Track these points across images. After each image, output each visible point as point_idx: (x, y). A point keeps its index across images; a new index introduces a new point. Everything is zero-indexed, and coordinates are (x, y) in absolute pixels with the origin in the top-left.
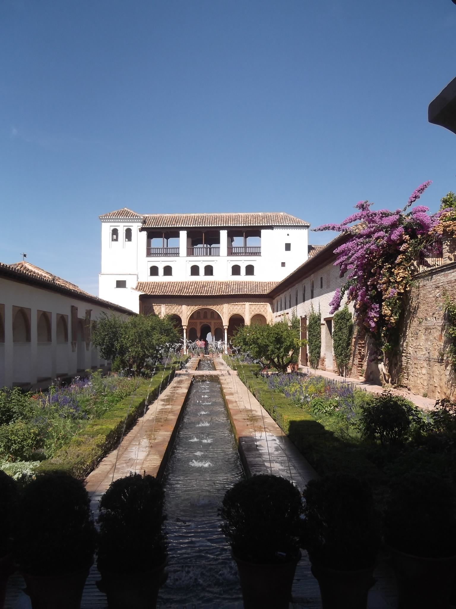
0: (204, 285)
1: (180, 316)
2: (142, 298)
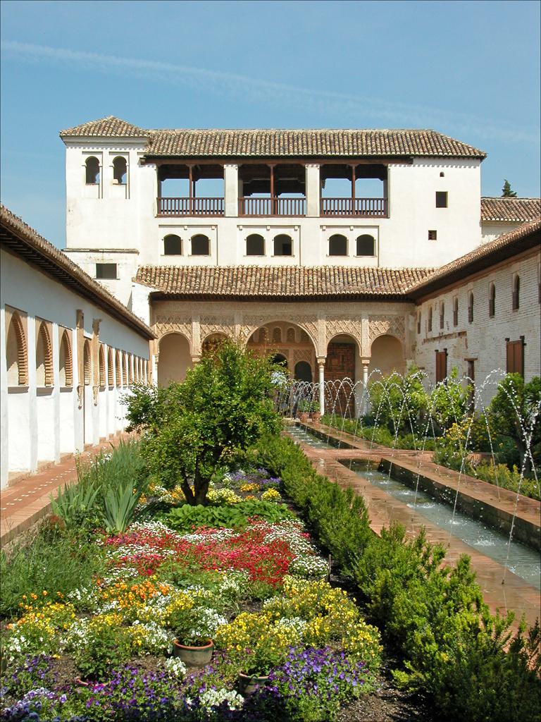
0: (272, 275)
2: (155, 299)
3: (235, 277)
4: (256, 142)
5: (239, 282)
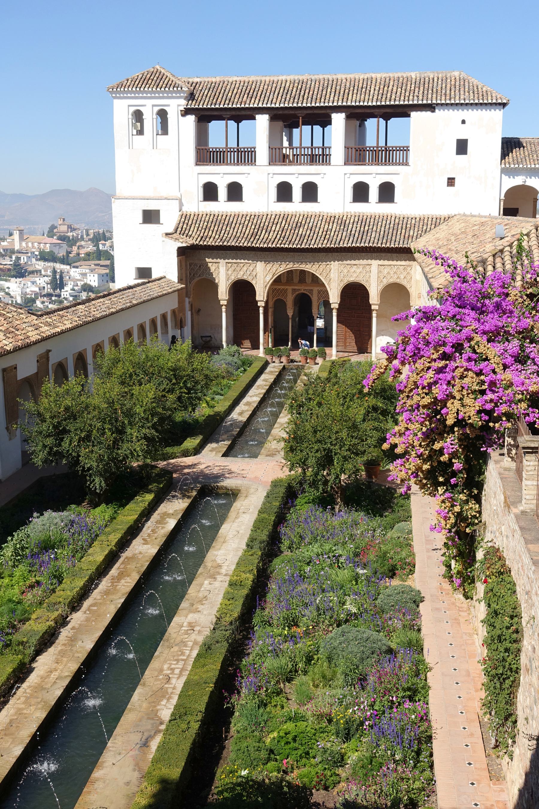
1: (253, 283)
3: (262, 225)
5: (264, 231)
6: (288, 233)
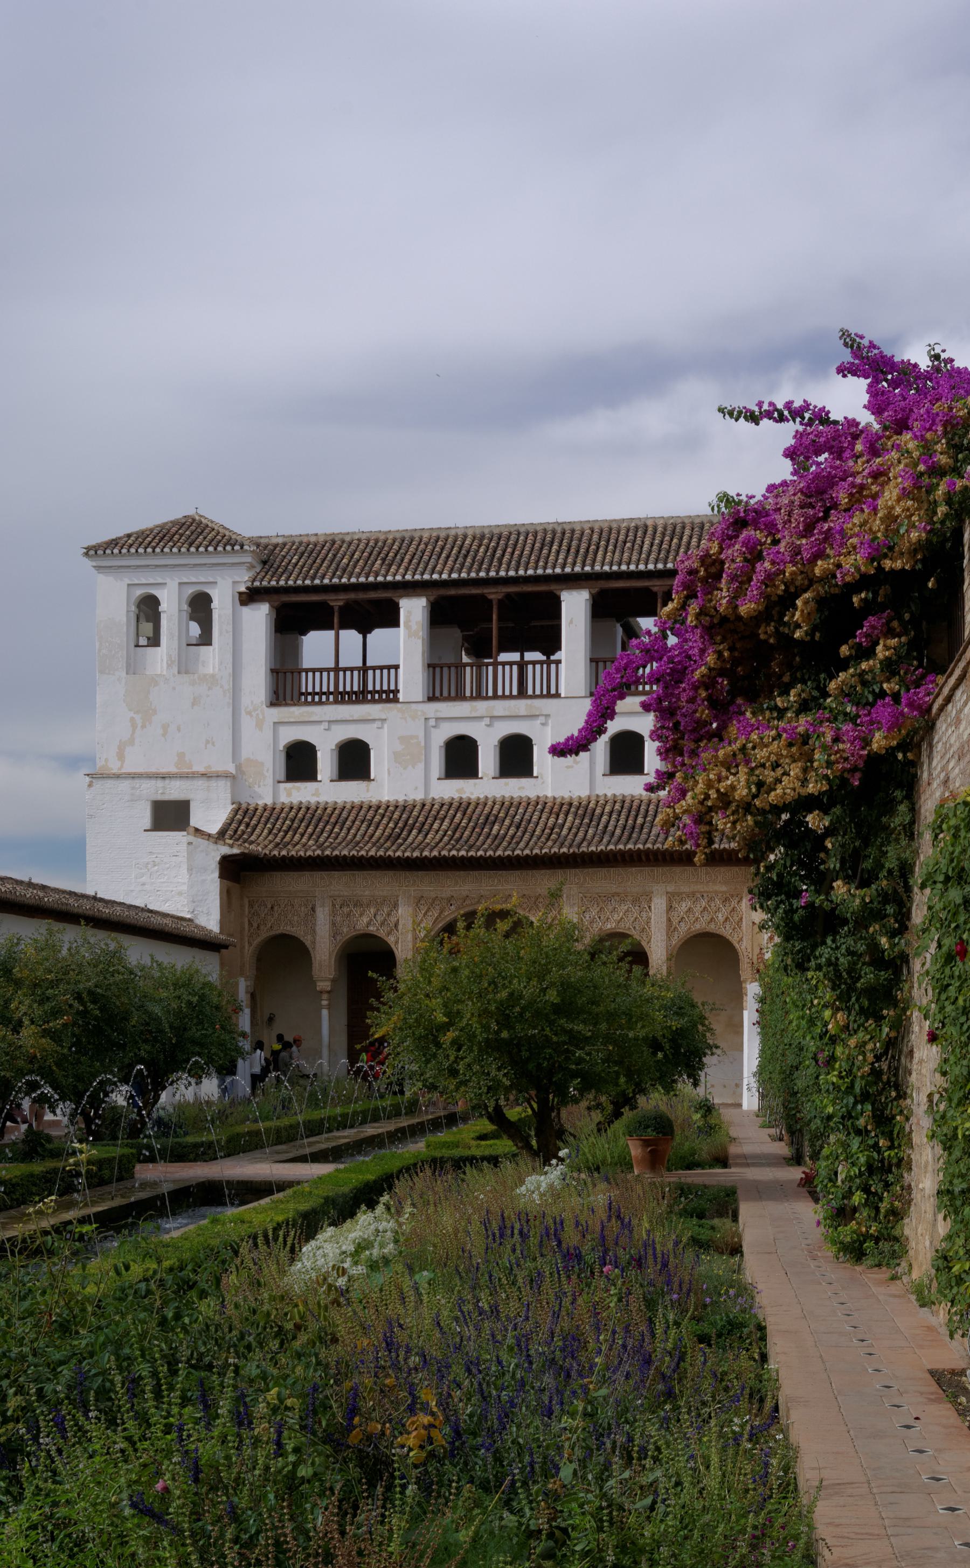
1: (391, 940)
3: (411, 822)
4: (468, 552)
5: (414, 832)
6: (467, 833)
